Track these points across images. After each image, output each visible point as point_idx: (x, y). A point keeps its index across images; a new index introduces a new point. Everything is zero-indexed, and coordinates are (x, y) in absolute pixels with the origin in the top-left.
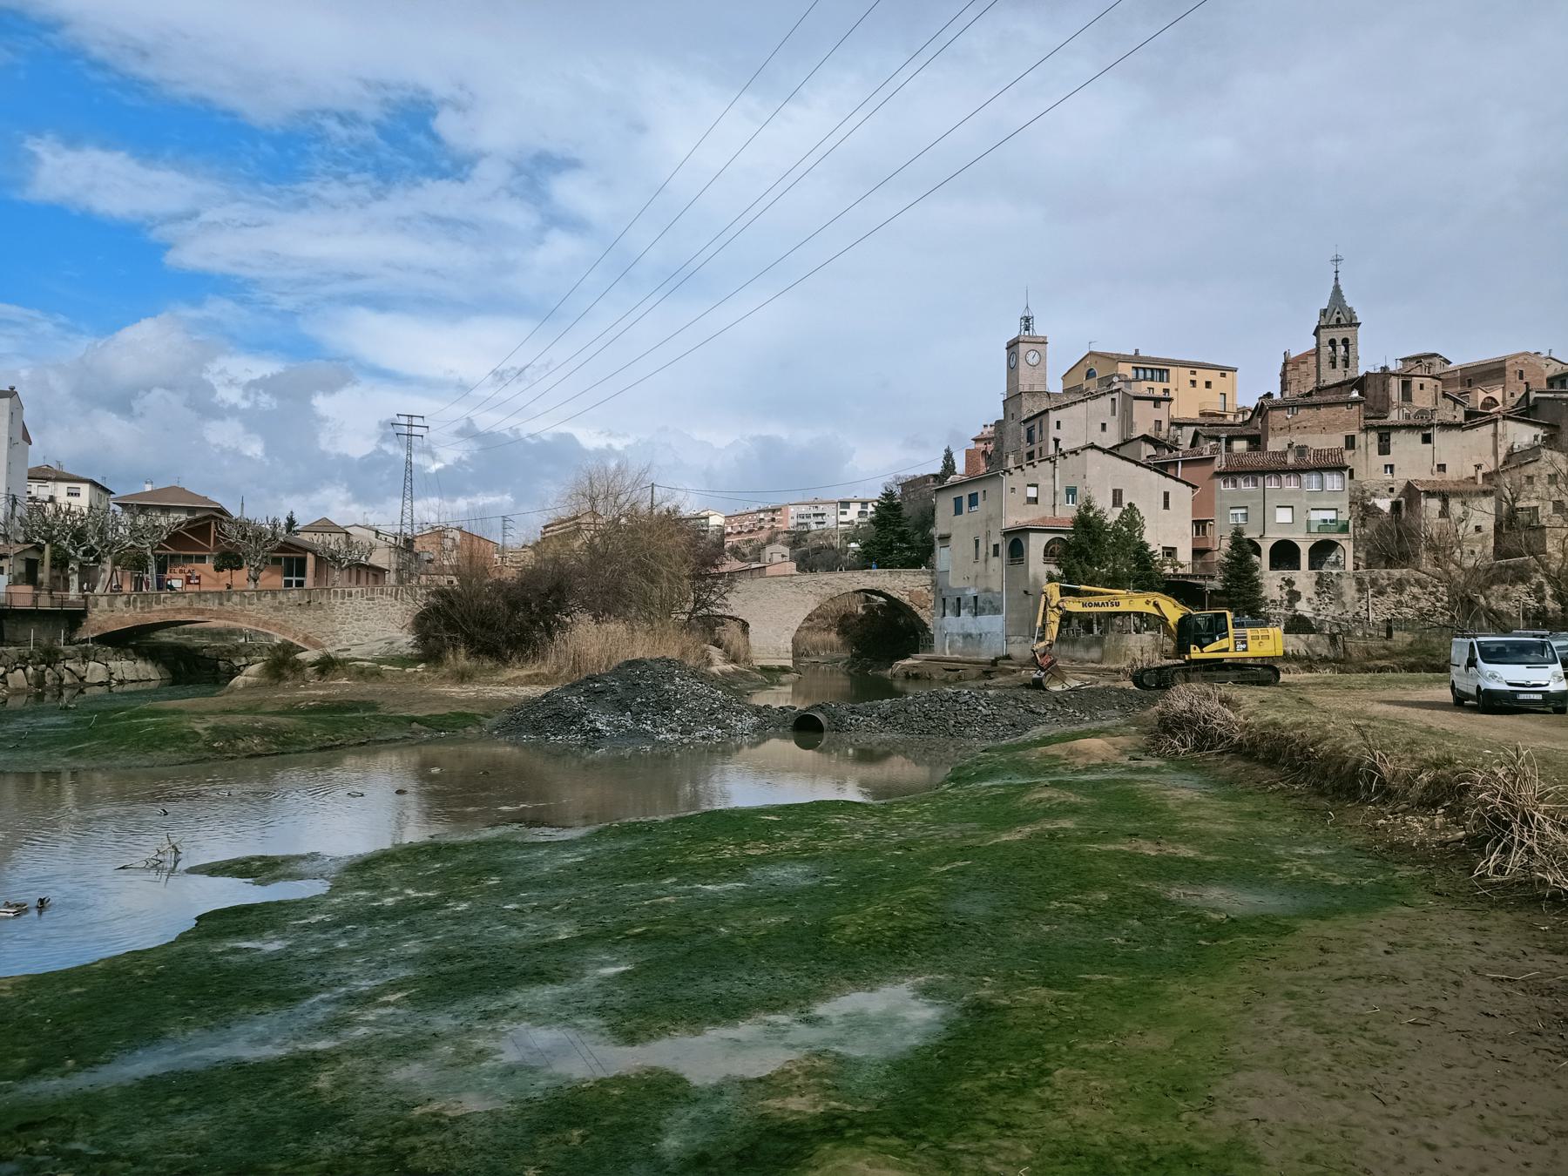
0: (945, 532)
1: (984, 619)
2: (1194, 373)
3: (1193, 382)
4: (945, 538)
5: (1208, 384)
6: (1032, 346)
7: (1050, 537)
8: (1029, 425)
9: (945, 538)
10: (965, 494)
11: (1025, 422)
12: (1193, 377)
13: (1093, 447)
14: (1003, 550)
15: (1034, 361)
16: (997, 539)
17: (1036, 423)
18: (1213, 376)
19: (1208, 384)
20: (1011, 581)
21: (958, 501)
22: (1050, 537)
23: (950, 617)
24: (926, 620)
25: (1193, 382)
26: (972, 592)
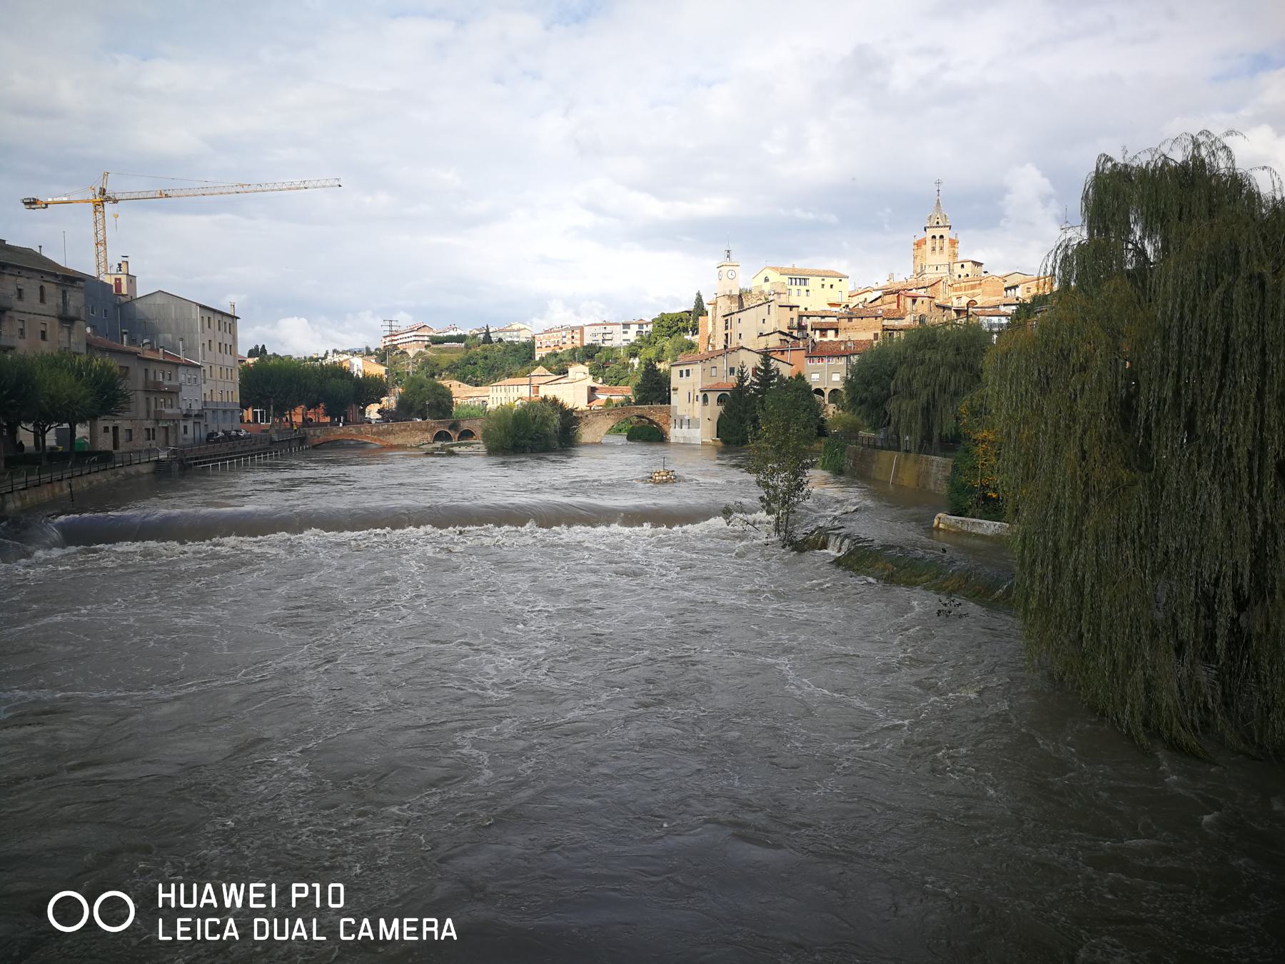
0: (676, 387)
1: (692, 430)
2: (823, 280)
3: (823, 285)
4: (675, 389)
5: (832, 286)
6: (731, 268)
7: (720, 393)
8: (726, 318)
9: (675, 389)
10: (684, 368)
11: (724, 316)
12: (823, 283)
13: (742, 348)
14: (700, 398)
15: (732, 277)
16: (698, 393)
17: (729, 318)
18: (835, 281)
19: (832, 286)
20: (703, 413)
21: (681, 372)
22: (720, 393)
23: (678, 429)
24: (667, 430)
25: (823, 285)
26: (687, 418)
